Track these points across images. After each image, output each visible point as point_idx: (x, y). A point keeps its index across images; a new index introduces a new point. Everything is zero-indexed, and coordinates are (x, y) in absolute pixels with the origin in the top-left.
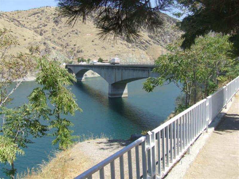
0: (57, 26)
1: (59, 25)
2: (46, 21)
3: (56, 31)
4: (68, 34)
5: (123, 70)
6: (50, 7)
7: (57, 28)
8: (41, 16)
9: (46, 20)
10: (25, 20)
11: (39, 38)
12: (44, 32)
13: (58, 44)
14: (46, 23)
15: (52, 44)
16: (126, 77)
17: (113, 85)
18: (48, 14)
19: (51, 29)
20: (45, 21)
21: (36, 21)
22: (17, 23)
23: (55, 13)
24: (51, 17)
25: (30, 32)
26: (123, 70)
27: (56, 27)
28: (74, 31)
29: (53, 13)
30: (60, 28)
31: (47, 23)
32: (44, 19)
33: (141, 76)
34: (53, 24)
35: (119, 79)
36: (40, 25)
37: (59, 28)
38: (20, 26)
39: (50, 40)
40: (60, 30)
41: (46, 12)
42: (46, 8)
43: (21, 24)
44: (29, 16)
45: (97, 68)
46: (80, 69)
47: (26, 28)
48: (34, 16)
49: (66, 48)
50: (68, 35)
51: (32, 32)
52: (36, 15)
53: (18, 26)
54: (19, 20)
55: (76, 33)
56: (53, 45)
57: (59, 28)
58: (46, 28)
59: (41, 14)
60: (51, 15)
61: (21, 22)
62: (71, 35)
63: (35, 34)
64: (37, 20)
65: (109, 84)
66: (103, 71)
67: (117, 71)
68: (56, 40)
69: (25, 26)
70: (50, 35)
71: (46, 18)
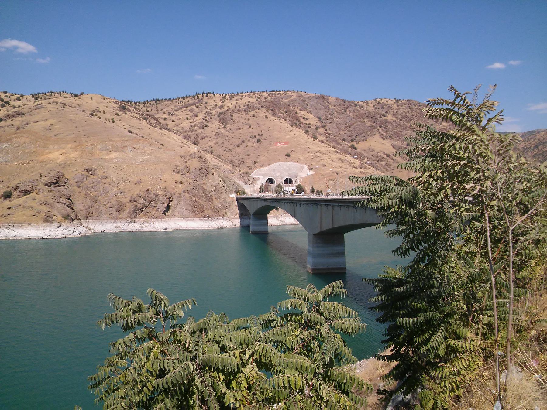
0: (225, 127)
1: (229, 126)
2: (205, 118)
3: (223, 136)
4: (243, 142)
5: (336, 208)
6: (213, 93)
7: (223, 131)
8: (196, 109)
9: (206, 117)
10: (169, 116)
11: (194, 149)
12: (203, 138)
13: (225, 161)
14: (206, 123)
15: (214, 159)
16: (341, 222)
17: (316, 235)
18: (209, 107)
19: (214, 133)
20: (203, 119)
21: (187, 119)
22: (153, 121)
23: (221, 104)
24: (214, 111)
25: (176, 137)
26: (336, 208)
27: (223, 129)
28: (255, 137)
29: (219, 106)
30: (230, 131)
31: (208, 122)
32: (201, 116)
33: (370, 221)
34: (217, 124)
35: (327, 225)
36: (195, 125)
37: (229, 131)
38: (158, 127)
39: (212, 153)
40: (231, 135)
41: (206, 103)
42: (207, 96)
43: (160, 123)
44: (176, 111)
45: (289, 204)
46: (260, 204)
47: (169, 130)
48: (185, 111)
49: (239, 167)
50: (244, 144)
51: (178, 139)
52: (189, 108)
53: (156, 127)
54: (157, 116)
55: (259, 141)
56: (216, 161)
57: (229, 131)
58: (206, 132)
59: (197, 107)
60: (214, 109)
61: (161, 120)
62: (249, 144)
63: (186, 141)
64: (189, 117)
65: (309, 234)
66: (299, 209)
67: (324, 207)
68: (222, 152)
69: (169, 127)
70: (212, 144)
71: (205, 114)
